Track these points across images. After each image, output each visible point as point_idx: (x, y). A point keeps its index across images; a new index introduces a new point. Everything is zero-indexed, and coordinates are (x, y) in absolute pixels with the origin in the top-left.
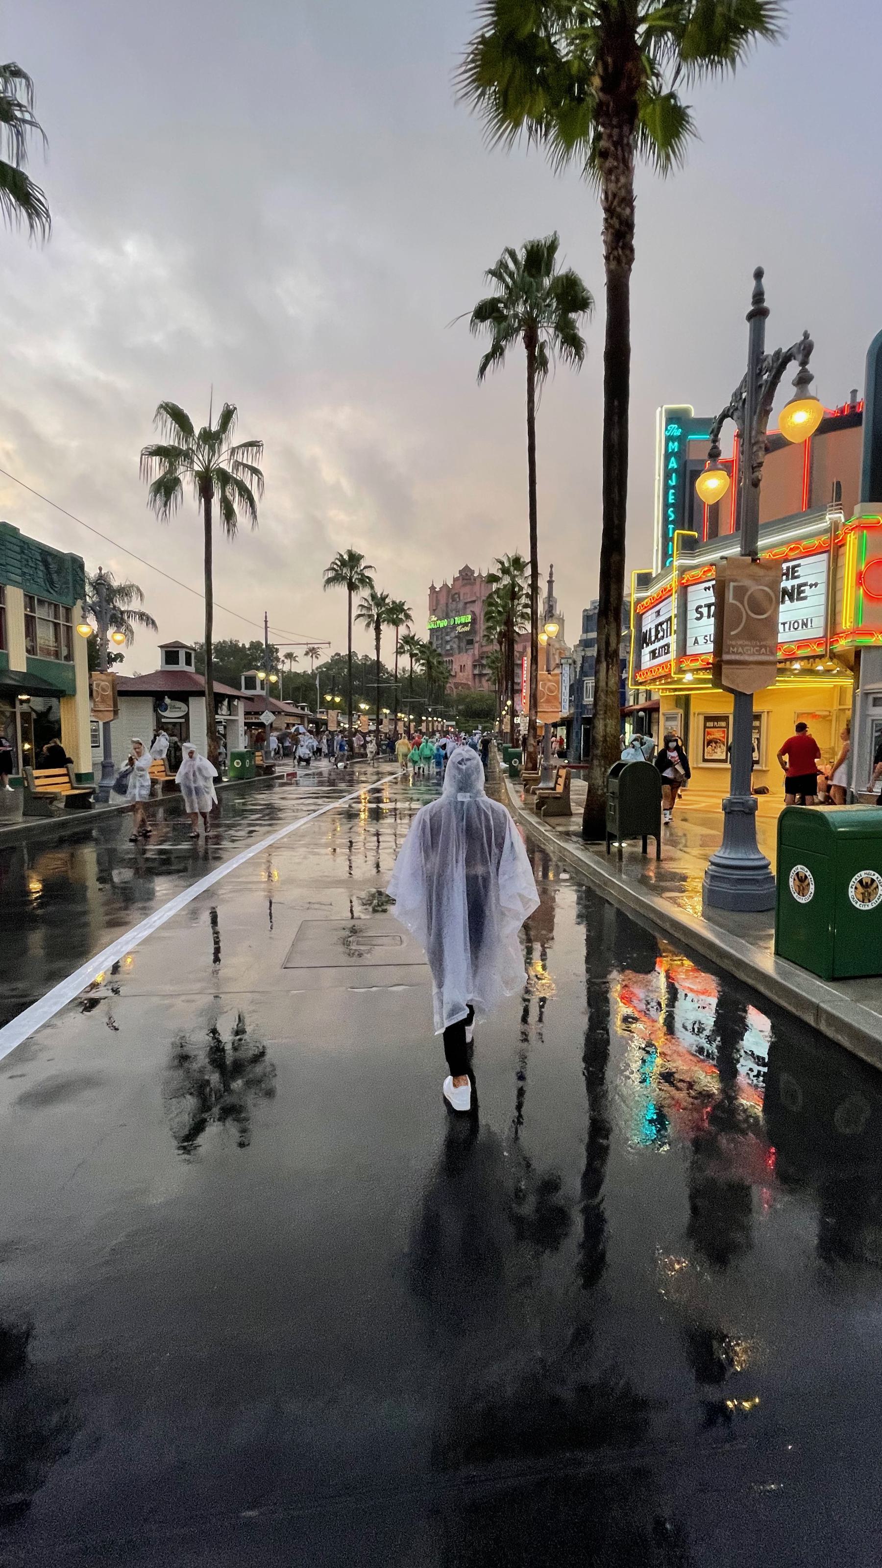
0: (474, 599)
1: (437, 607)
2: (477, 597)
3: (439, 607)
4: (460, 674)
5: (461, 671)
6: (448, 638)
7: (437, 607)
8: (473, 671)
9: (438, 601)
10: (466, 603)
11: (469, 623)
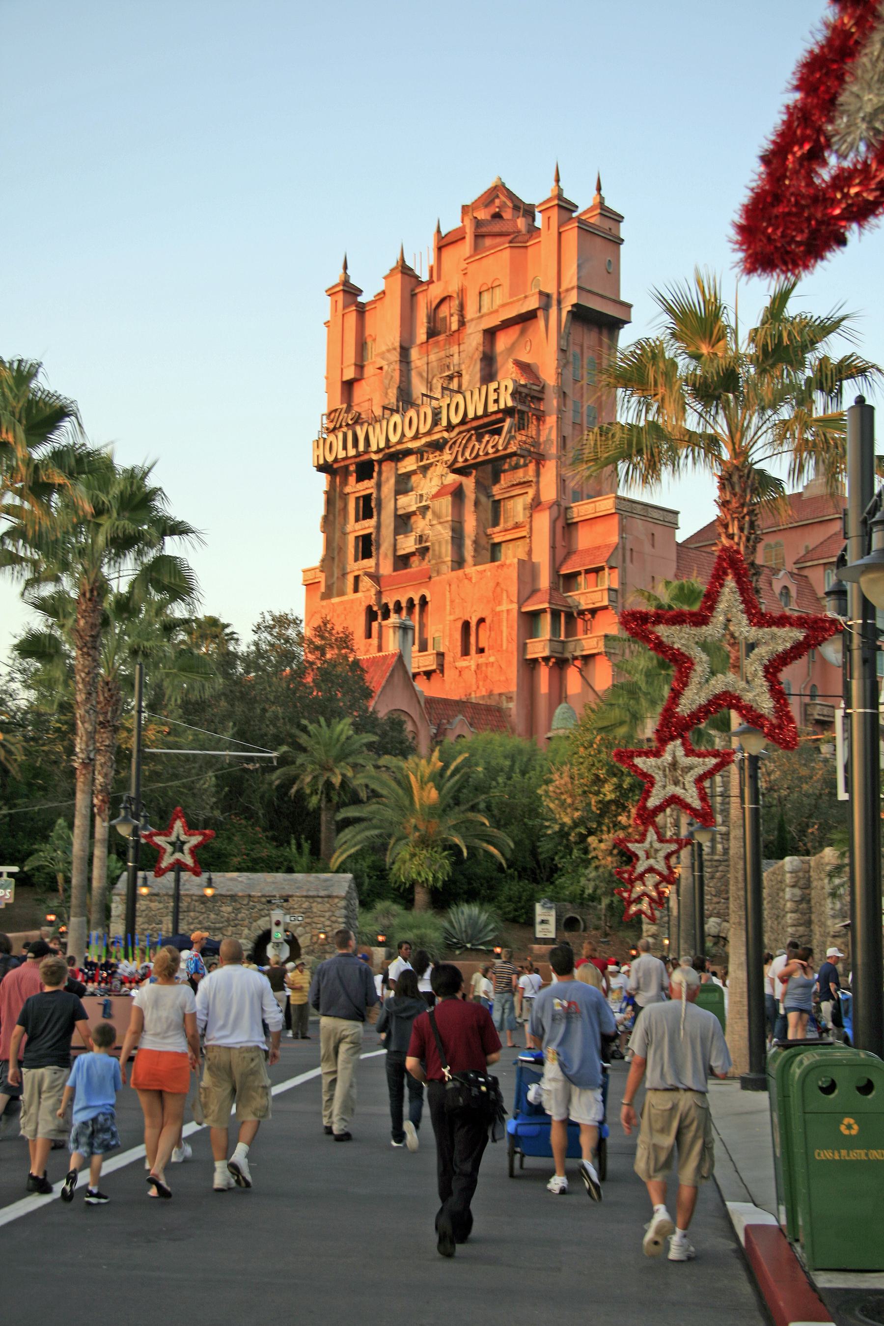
0: (533, 303)
1: (360, 367)
2: (545, 296)
3: (369, 370)
4: (462, 663)
5: (466, 652)
6: (409, 503)
7: (360, 367)
8: (523, 648)
9: (362, 346)
10: (491, 334)
11: (508, 412)
